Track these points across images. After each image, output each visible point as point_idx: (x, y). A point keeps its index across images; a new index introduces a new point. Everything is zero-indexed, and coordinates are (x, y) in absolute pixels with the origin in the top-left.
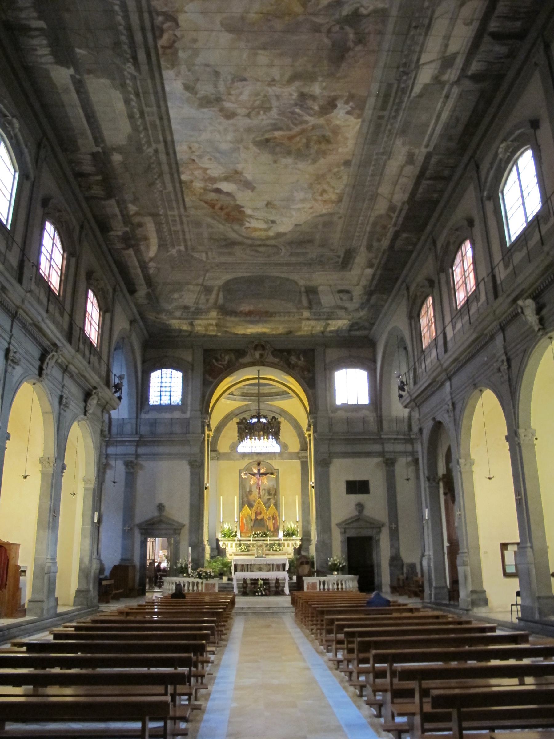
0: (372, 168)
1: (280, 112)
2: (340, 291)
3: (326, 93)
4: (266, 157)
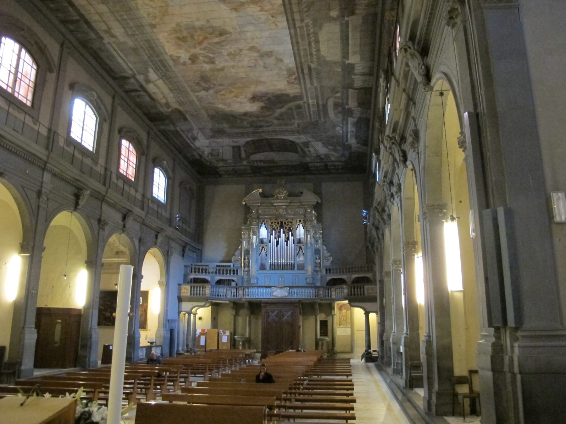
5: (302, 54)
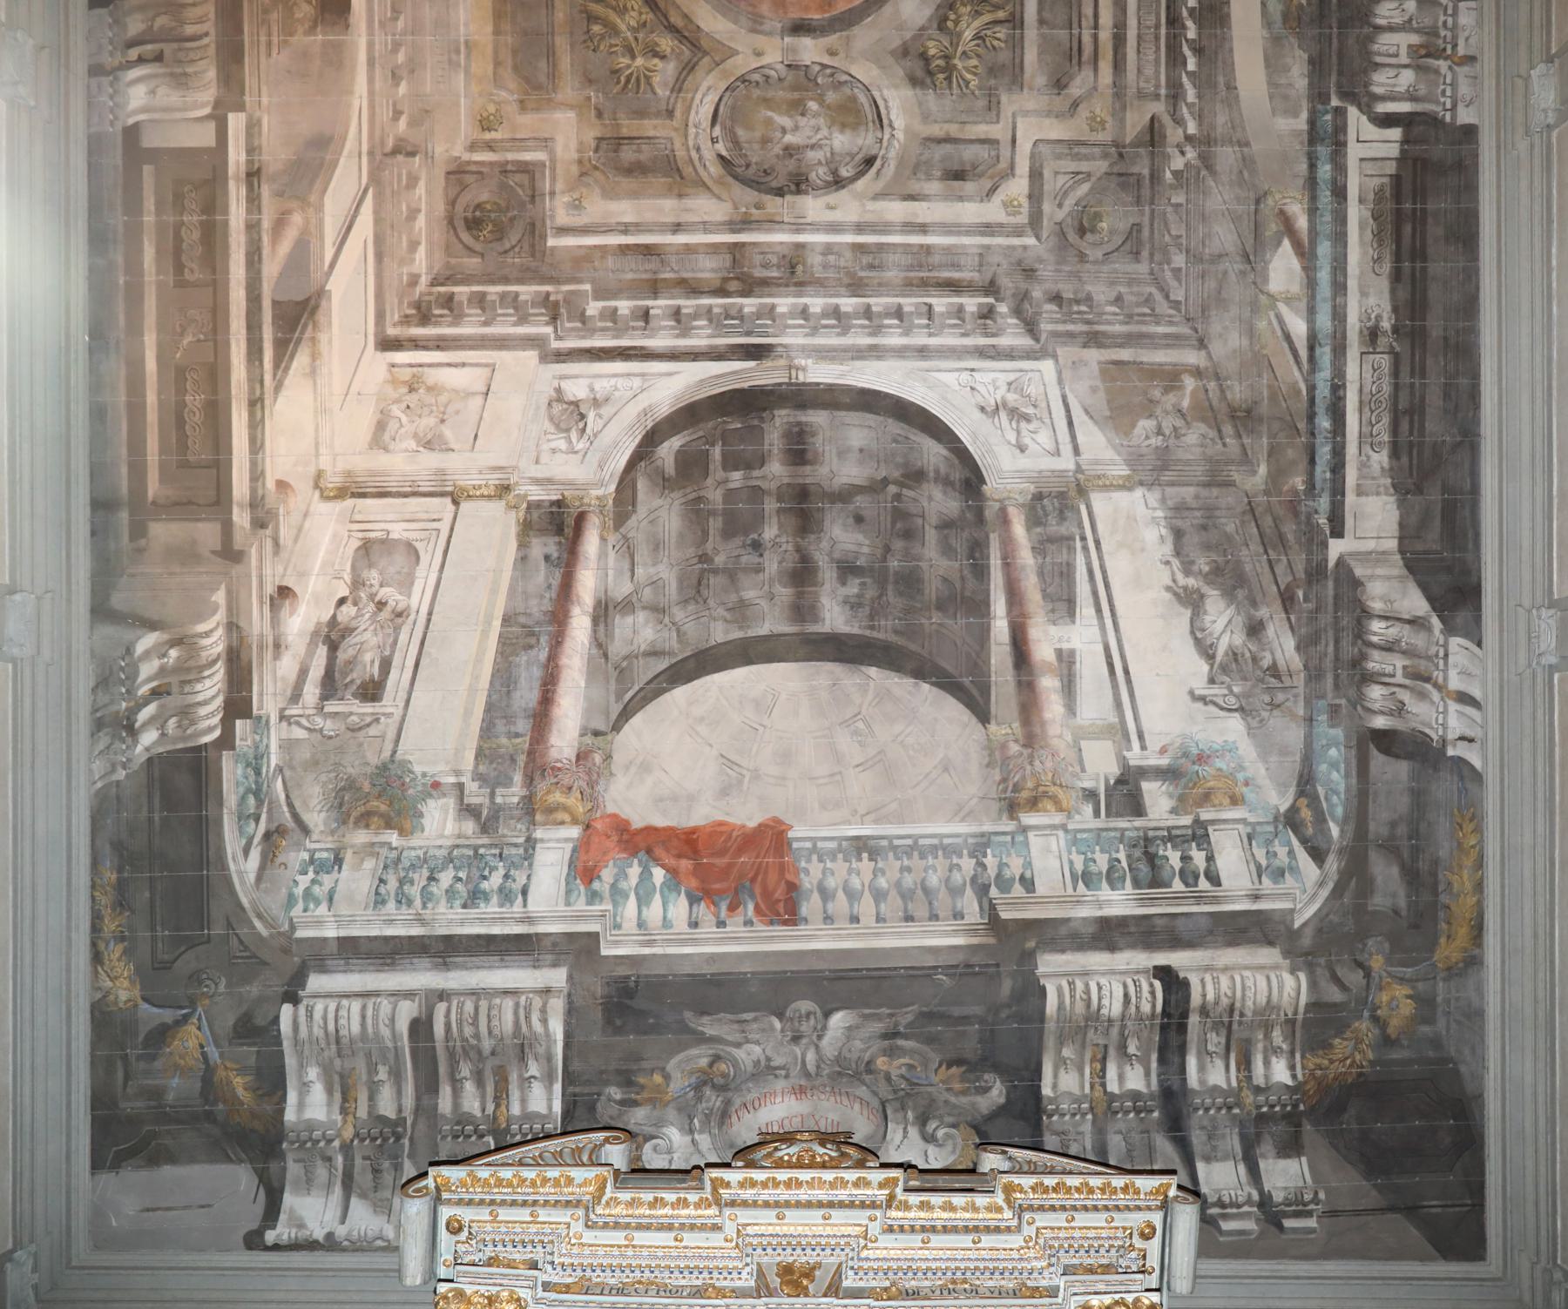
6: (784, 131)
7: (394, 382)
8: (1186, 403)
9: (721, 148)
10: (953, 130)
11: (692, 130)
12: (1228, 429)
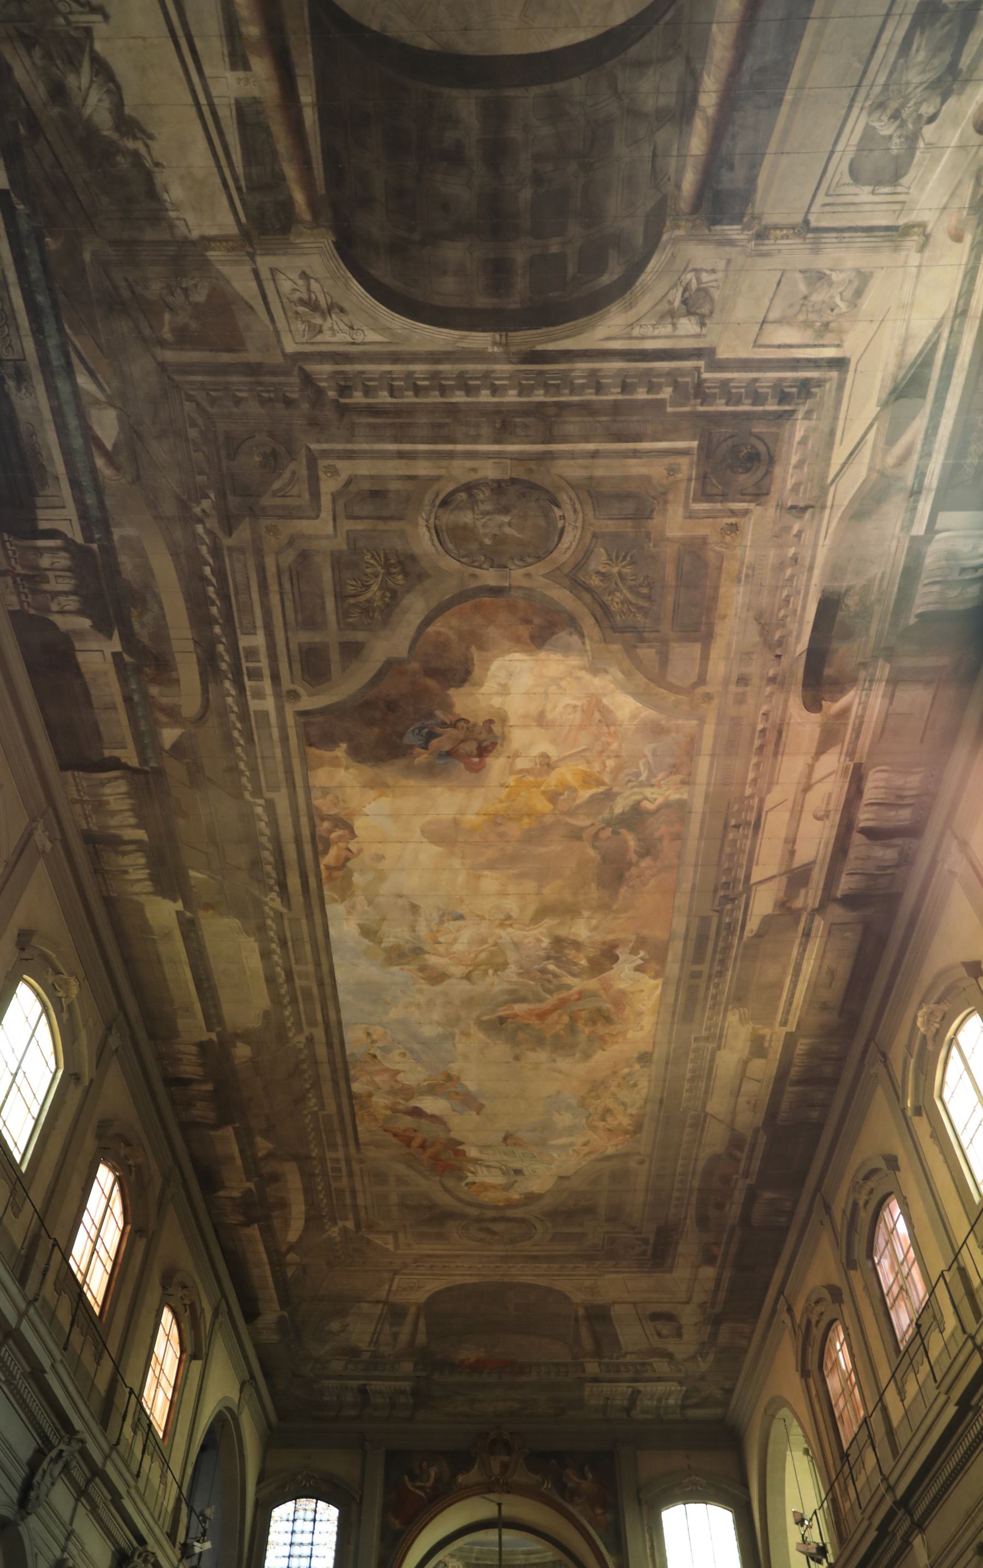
0: (690, 1066)
1: (521, 971)
2: (655, 1317)
3: (599, 937)
4: (500, 1049)
5: (308, 948)
6: (510, 524)
7: (841, 332)
8: (167, 316)
9: (558, 512)
10: (381, 525)
11: (579, 524)
12: (126, 294)
